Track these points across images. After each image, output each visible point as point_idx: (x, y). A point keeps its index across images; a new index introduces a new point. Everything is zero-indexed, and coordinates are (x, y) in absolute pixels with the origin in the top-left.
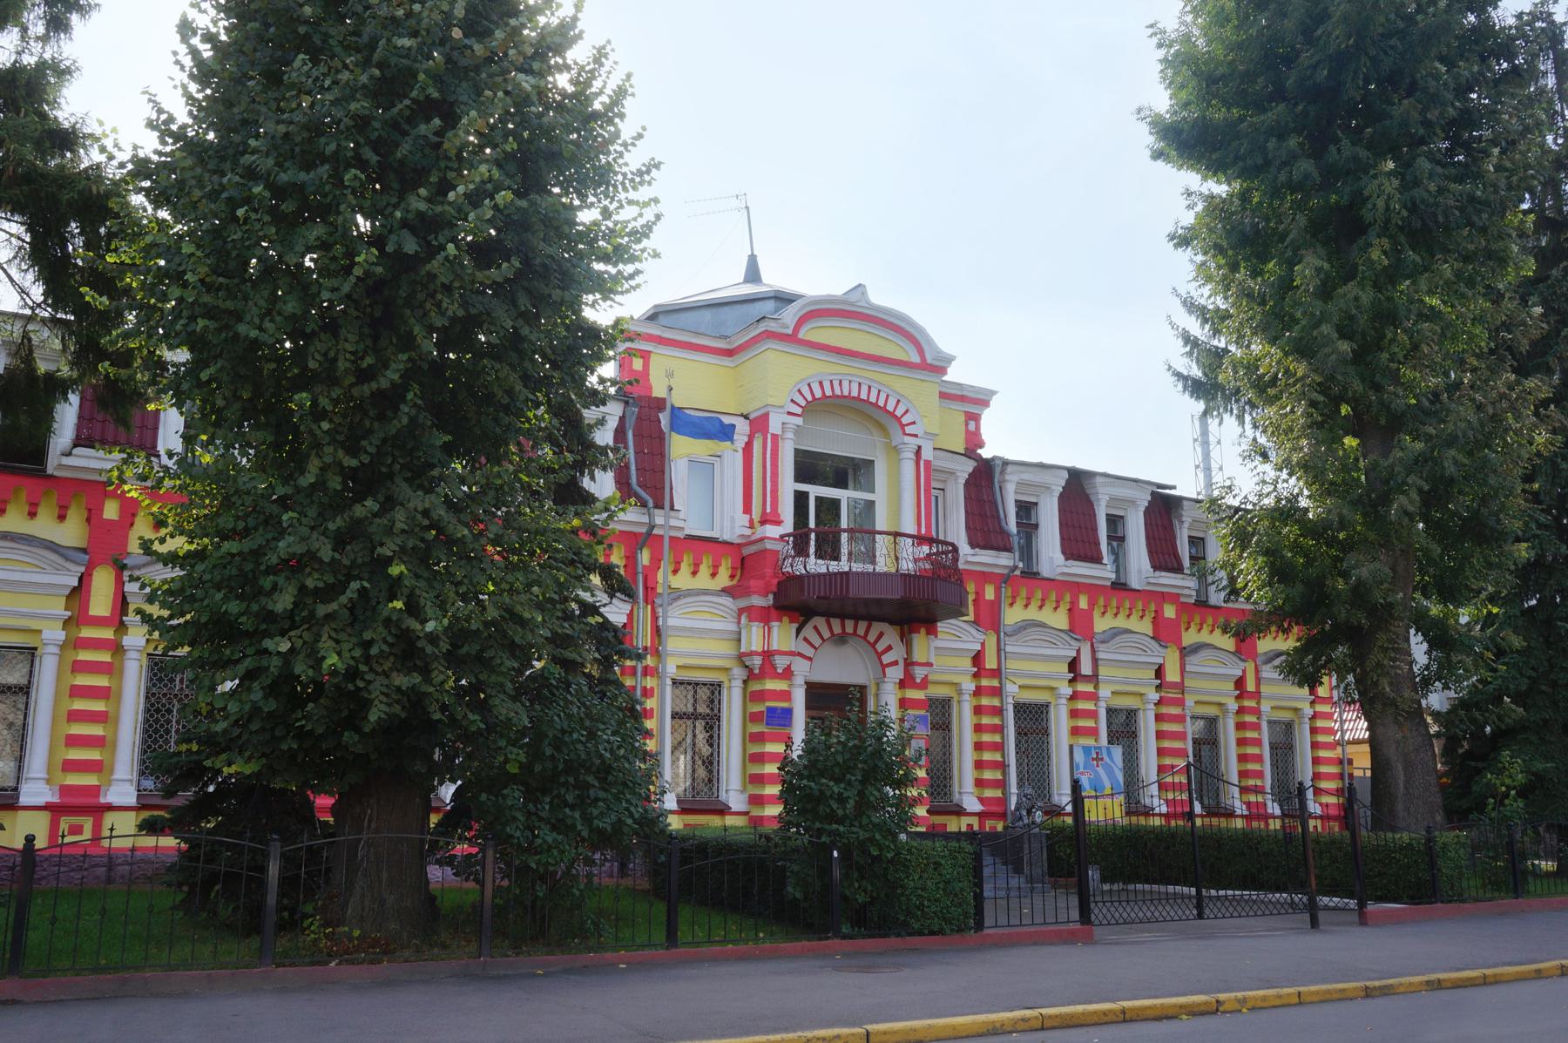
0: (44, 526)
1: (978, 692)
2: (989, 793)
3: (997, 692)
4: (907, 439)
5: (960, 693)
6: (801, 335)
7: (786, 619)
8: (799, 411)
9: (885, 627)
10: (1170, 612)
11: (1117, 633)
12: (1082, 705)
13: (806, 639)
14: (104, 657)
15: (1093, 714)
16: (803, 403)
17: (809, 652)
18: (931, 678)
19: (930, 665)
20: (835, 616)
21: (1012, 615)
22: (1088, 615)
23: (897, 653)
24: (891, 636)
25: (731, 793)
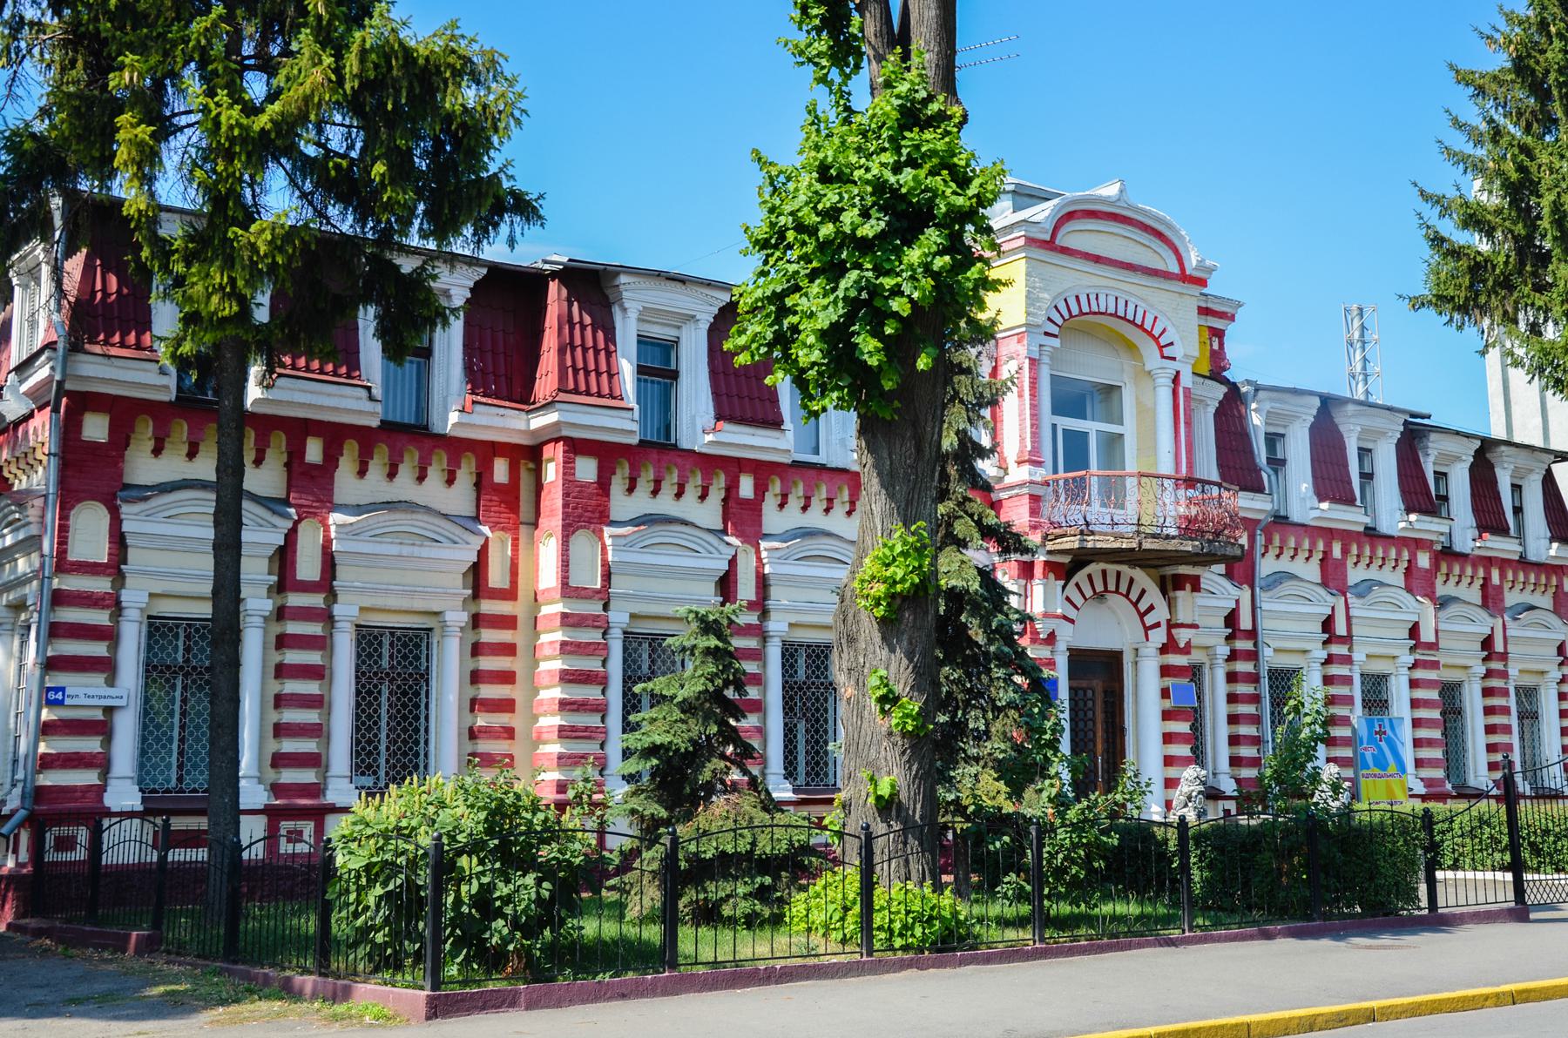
0: (434, 491)
1: (1233, 656)
2: (1248, 773)
3: (1253, 656)
5: (1212, 657)
6: (1061, 240)
8: (1055, 330)
10: (1424, 560)
11: (1281, 577)
12: (1335, 670)
13: (1068, 599)
14: (315, 629)
15: (1347, 680)
16: (1059, 321)
17: (1072, 613)
18: (1193, 643)
19: (1195, 626)
21: (1266, 566)
22: (1341, 564)
23: (1161, 614)
25: (1221, 777)
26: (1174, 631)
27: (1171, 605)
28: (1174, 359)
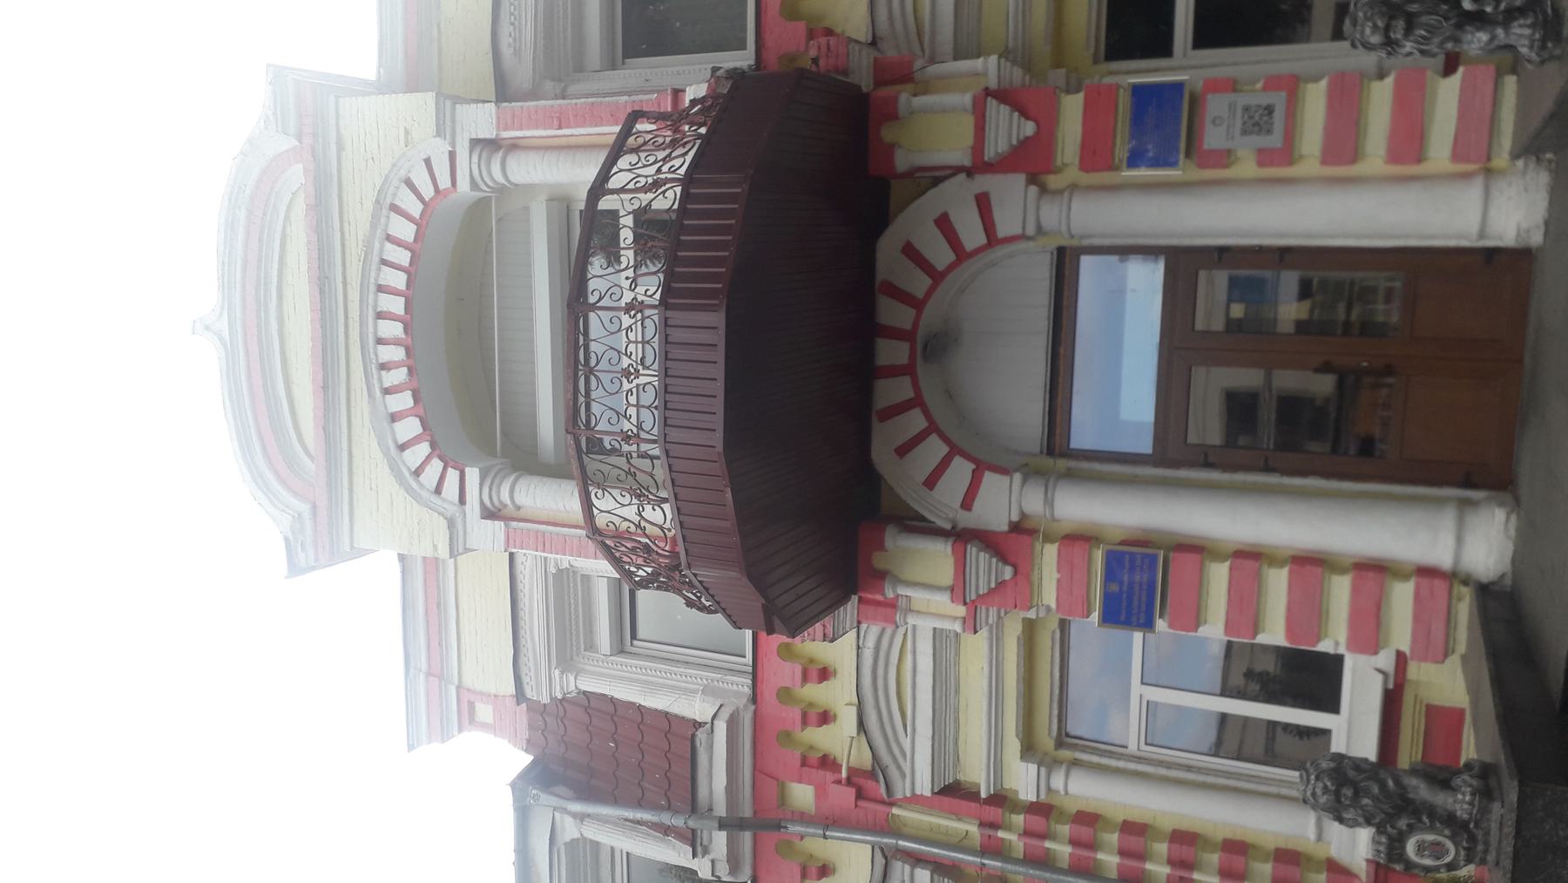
4: (464, 185)
7: (879, 561)
20: (867, 393)
23: (957, 200)
24: (914, 224)
26: (990, 154)
27: (935, 177)
28: (452, 156)
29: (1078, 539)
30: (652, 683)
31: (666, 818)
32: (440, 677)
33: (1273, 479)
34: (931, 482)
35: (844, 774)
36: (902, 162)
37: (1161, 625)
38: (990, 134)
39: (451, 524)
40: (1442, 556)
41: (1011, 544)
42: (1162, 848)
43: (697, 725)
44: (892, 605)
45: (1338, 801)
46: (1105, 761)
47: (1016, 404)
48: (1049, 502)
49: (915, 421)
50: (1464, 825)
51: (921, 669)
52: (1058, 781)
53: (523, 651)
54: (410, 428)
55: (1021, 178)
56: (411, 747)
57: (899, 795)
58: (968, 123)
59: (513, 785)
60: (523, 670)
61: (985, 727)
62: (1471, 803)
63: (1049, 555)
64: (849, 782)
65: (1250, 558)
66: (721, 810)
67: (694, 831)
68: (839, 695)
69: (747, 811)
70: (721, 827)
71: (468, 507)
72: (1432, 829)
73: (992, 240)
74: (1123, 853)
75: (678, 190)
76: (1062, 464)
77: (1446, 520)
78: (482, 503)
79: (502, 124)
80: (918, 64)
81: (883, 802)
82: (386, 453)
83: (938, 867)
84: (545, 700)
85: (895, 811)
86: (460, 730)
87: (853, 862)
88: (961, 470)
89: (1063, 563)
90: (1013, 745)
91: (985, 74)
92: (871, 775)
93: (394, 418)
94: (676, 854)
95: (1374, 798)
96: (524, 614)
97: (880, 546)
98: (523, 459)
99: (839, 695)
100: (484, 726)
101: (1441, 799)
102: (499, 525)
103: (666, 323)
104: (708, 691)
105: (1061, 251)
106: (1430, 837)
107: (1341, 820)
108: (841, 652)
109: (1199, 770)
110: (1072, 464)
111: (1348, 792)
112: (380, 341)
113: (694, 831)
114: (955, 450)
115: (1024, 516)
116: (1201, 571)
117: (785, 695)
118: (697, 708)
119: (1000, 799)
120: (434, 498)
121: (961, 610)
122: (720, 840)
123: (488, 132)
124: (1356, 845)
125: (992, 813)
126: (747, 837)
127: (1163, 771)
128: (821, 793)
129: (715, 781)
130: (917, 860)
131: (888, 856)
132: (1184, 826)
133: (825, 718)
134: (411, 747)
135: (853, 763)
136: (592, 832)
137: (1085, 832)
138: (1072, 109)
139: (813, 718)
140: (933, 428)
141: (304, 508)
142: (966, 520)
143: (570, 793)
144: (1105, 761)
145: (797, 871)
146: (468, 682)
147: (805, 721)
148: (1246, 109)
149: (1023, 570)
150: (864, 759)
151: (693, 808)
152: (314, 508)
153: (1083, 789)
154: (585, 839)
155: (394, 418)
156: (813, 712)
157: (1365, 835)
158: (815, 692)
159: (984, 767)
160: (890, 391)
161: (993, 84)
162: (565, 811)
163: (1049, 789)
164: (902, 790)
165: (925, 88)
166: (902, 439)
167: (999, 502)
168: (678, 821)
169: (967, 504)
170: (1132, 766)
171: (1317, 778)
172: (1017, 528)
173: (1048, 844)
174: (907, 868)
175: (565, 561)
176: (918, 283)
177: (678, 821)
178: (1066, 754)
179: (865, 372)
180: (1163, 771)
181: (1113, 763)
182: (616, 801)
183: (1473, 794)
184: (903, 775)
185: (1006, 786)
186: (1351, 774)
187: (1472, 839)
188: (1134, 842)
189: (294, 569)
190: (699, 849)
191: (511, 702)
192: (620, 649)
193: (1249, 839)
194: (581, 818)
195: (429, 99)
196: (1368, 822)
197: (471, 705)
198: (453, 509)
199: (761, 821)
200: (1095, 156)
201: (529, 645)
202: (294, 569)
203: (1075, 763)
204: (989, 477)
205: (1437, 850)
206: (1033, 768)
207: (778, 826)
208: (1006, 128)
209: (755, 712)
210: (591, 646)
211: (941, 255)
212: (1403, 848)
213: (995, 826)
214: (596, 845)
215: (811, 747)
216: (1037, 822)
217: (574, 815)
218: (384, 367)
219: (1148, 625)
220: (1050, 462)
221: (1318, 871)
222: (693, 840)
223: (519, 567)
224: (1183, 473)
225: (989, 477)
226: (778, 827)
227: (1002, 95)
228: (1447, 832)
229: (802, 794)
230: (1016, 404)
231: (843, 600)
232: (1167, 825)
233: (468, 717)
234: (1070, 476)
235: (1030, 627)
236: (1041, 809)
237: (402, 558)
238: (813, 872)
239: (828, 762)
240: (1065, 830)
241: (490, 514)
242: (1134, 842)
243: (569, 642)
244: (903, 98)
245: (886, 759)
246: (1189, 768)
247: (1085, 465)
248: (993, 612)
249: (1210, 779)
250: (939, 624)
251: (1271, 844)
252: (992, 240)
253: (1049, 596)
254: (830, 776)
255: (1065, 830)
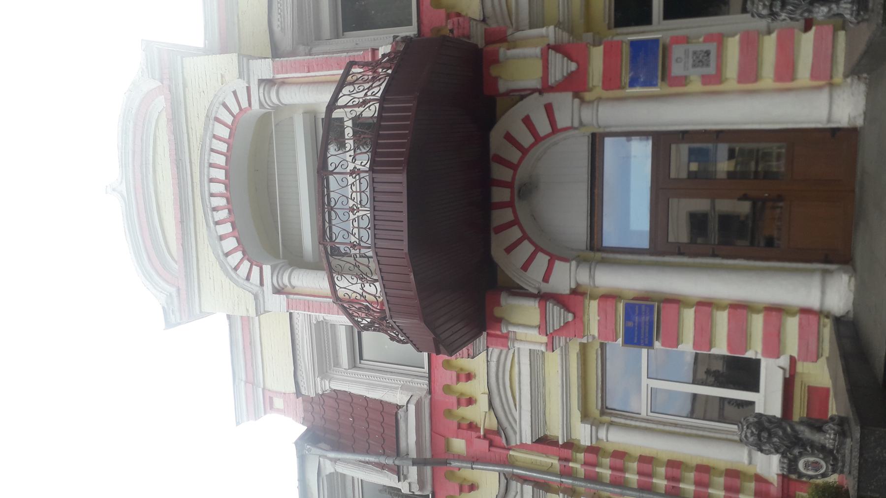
4: (255, 106)
7: (497, 312)
8: (256, 270)
9: (496, 136)
20: (488, 219)
23: (534, 107)
24: (510, 122)
26: (552, 81)
27: (521, 95)
28: (248, 89)
29: (609, 297)
30: (373, 384)
31: (382, 460)
32: (253, 384)
33: (718, 261)
34: (525, 267)
35: (482, 433)
36: (502, 87)
37: (657, 344)
38: (551, 71)
39: (256, 297)
40: (813, 300)
41: (572, 301)
42: (662, 470)
43: (398, 407)
44: (506, 337)
45: (760, 440)
46: (628, 422)
47: (572, 222)
48: (592, 277)
49: (515, 233)
50: (831, 452)
51: (523, 372)
52: (602, 434)
53: (299, 368)
54: (231, 243)
55: (569, 95)
56: (238, 424)
57: (513, 444)
58: (539, 64)
59: (296, 443)
60: (300, 378)
61: (560, 404)
62: (834, 440)
63: (593, 307)
64: (485, 437)
65: (706, 306)
66: (413, 454)
67: (398, 467)
68: (477, 388)
69: (428, 455)
70: (414, 464)
71: (265, 288)
72: (813, 454)
73: (555, 130)
74: (640, 473)
75: (377, 105)
76: (599, 255)
77: (816, 280)
78: (273, 284)
79: (276, 71)
80: (509, 32)
81: (504, 448)
82: (218, 258)
83: (538, 485)
84: (313, 395)
85: (511, 453)
86: (265, 413)
87: (488, 480)
88: (542, 260)
89: (601, 311)
90: (576, 414)
91: (547, 36)
92: (497, 433)
93: (221, 238)
94: (388, 480)
95: (779, 437)
96: (299, 347)
97: (498, 304)
98: (295, 260)
99: (477, 388)
100: (279, 411)
101: (817, 438)
102: (283, 297)
103: (373, 181)
104: (404, 388)
105: (594, 135)
106: (812, 459)
107: (762, 451)
108: (478, 364)
109: (681, 426)
110: (604, 255)
111: (765, 435)
112: (212, 195)
113: (398, 467)
114: (538, 249)
115: (578, 285)
116: (679, 314)
117: (447, 389)
118: (398, 398)
119: (570, 445)
120: (246, 283)
121: (545, 339)
122: (413, 471)
123: (268, 76)
124: (770, 466)
125: (566, 453)
126: (428, 470)
127: (661, 427)
128: (469, 443)
129: (409, 439)
130: (525, 480)
131: (508, 479)
132: (675, 457)
133: (470, 401)
134: (238, 424)
135: (487, 426)
136: (341, 469)
137: (618, 462)
138: (597, 54)
139: (463, 401)
140: (525, 237)
141: (173, 290)
142: (546, 288)
143: (328, 447)
144: (628, 422)
145: (457, 489)
146: (269, 386)
147: (459, 403)
148: (695, 53)
149: (579, 315)
150: (493, 424)
151: (398, 454)
152: (179, 289)
153: (617, 438)
154: (337, 473)
155: (221, 238)
156: (463, 398)
157: (775, 459)
158: (465, 387)
159: (560, 427)
160: (501, 216)
161: (552, 41)
162: (326, 457)
163: (597, 439)
164: (515, 441)
165: (514, 45)
166: (508, 244)
167: (565, 277)
168: (390, 461)
169: (546, 279)
170: (643, 424)
171: (748, 428)
172: (574, 292)
173: (598, 470)
174: (519, 484)
175: (321, 316)
176: (514, 155)
177: (390, 461)
178: (606, 418)
179: (486, 206)
180: (661, 427)
181: (633, 423)
182: (354, 451)
183: (835, 434)
184: (515, 433)
185: (573, 437)
186: (766, 424)
187: (835, 459)
188: (646, 467)
189: (169, 325)
190: (402, 477)
191: (293, 397)
192: (354, 365)
193: (711, 465)
194: (335, 461)
195: (234, 56)
196: (777, 452)
197: (271, 399)
198: (257, 289)
199: (436, 460)
200: (611, 81)
201: (303, 364)
202: (169, 325)
203: (612, 424)
204: (558, 264)
205: (816, 466)
206: (588, 427)
207: (446, 463)
208: (560, 67)
209: (431, 399)
210: (337, 364)
211: (526, 139)
212: (797, 465)
213: (567, 460)
214: (344, 476)
215: (463, 418)
216: (591, 457)
217: (331, 459)
218: (214, 209)
219: (650, 345)
220: (591, 254)
221: (751, 481)
222: (398, 472)
223: (295, 321)
224: (667, 259)
225: (558, 264)
226: (446, 463)
227: (557, 48)
228: (821, 456)
229: (459, 445)
230: (572, 222)
231: (478, 335)
232: (665, 457)
233: (269, 406)
234: (603, 262)
235: (584, 348)
236: (593, 450)
237: (229, 317)
238: (466, 488)
239: (472, 426)
240: (607, 461)
241: (278, 291)
242: (646, 467)
243: (325, 363)
244: (502, 51)
245: (505, 424)
246: (676, 425)
247: (611, 256)
248: (563, 339)
249: (688, 431)
250: (533, 347)
251: (723, 467)
252: (555, 130)
253: (594, 330)
254: (474, 434)
255: (607, 461)
